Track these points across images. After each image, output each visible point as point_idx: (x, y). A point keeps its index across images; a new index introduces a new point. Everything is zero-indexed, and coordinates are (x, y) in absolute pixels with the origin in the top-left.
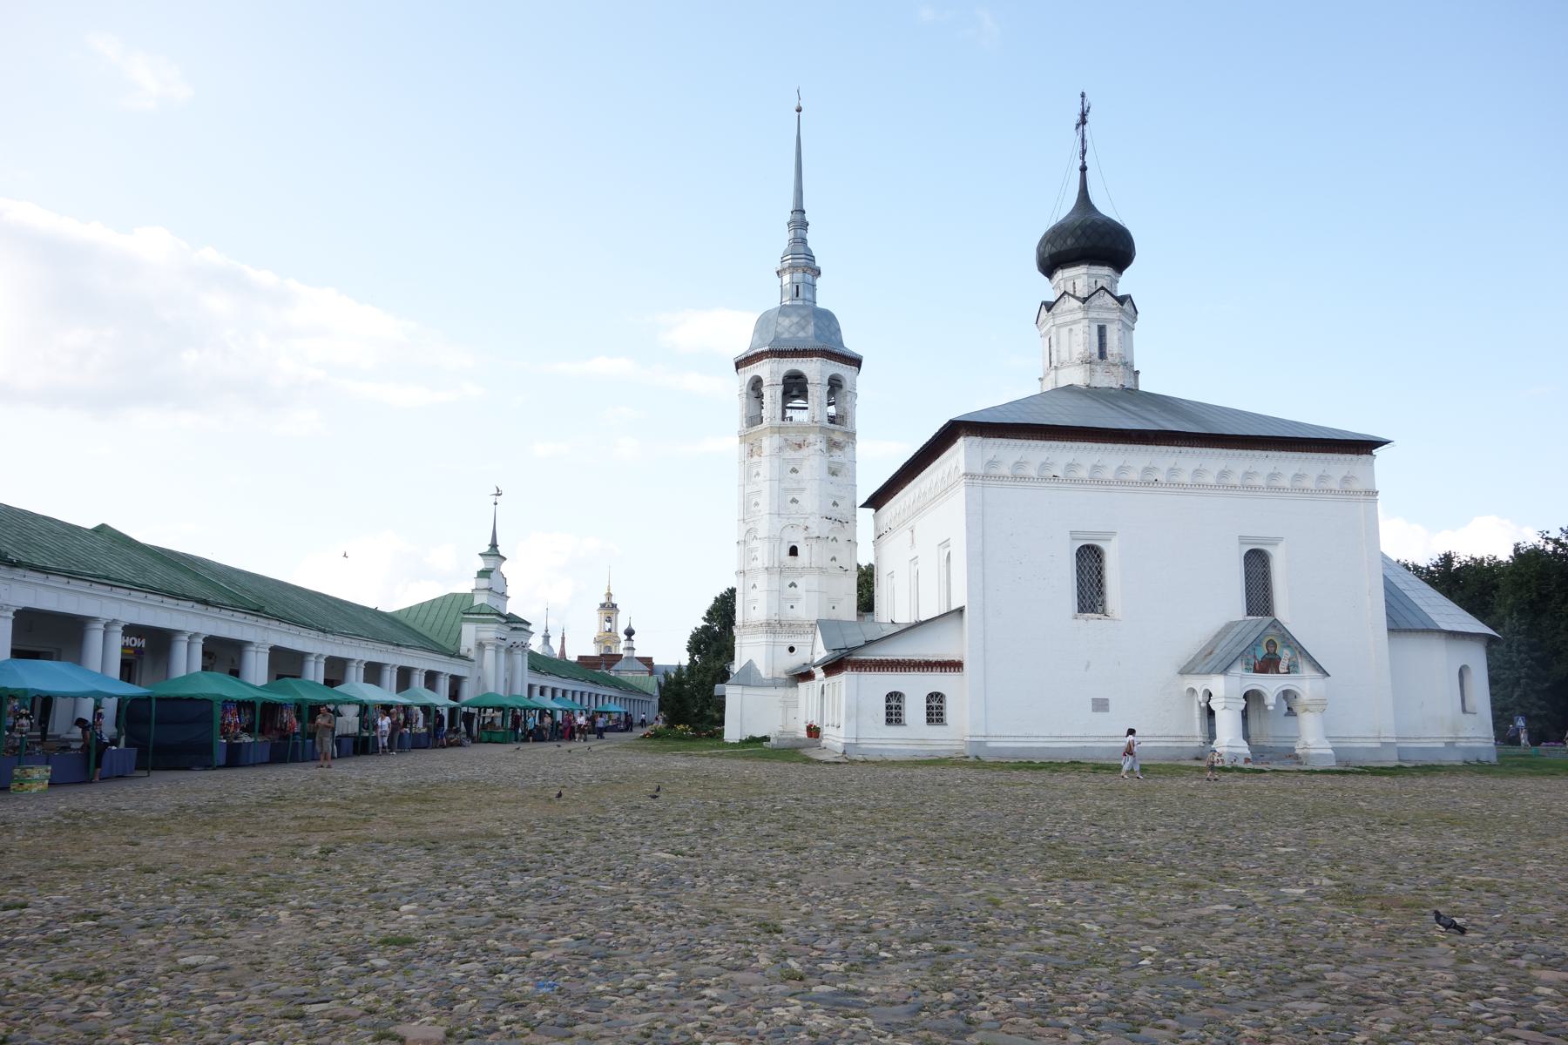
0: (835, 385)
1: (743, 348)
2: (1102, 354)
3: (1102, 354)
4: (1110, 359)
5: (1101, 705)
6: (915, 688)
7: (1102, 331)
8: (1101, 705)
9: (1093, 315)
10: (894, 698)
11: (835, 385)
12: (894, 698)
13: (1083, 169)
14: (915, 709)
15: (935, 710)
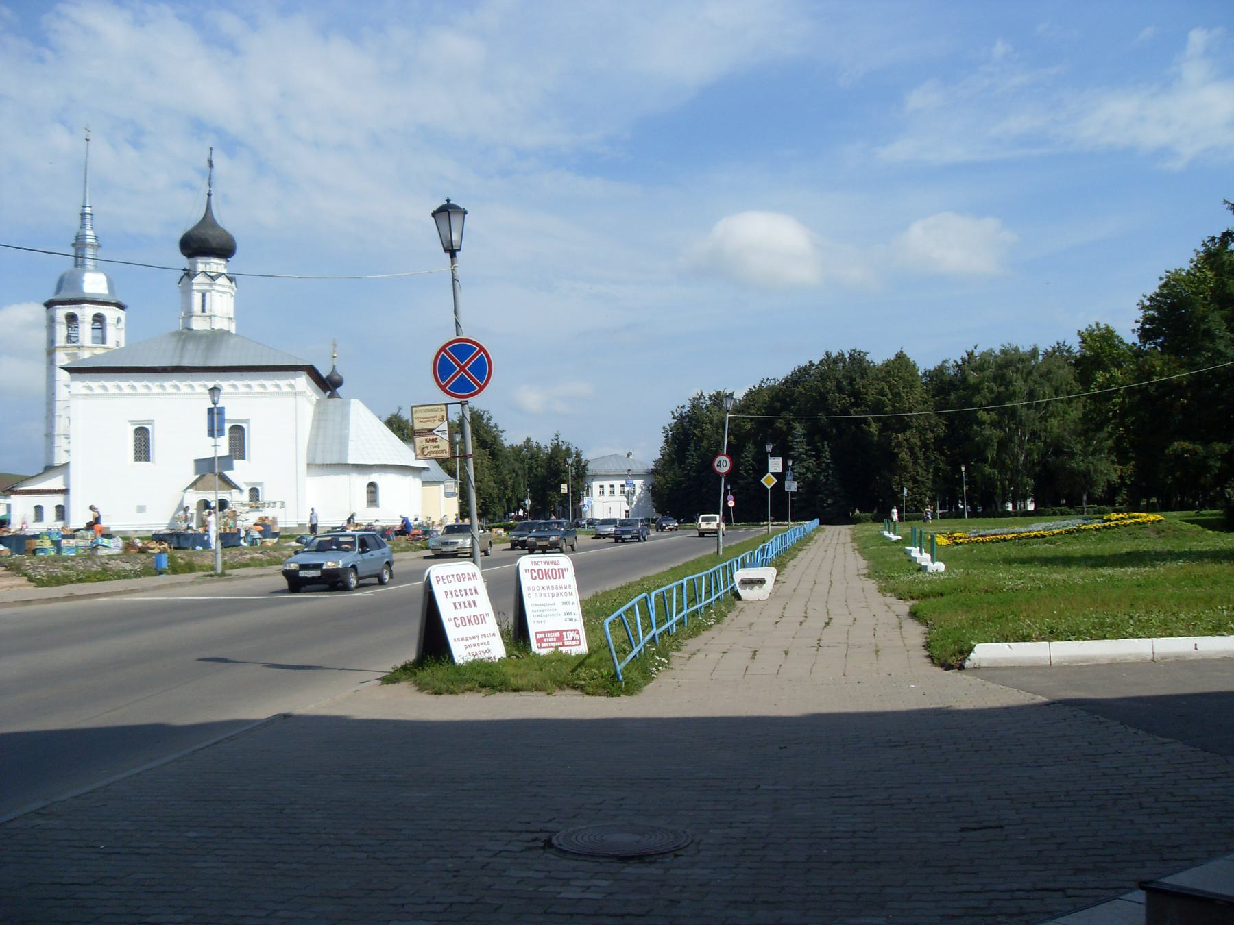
0: (99, 319)
1: (50, 296)
2: (203, 311)
3: (203, 311)
4: (208, 313)
5: (141, 509)
6: (50, 503)
7: (204, 296)
8: (141, 509)
9: (195, 287)
10: (39, 510)
11: (99, 319)
12: (39, 510)
13: (209, 195)
14: (50, 514)
15: (61, 512)
